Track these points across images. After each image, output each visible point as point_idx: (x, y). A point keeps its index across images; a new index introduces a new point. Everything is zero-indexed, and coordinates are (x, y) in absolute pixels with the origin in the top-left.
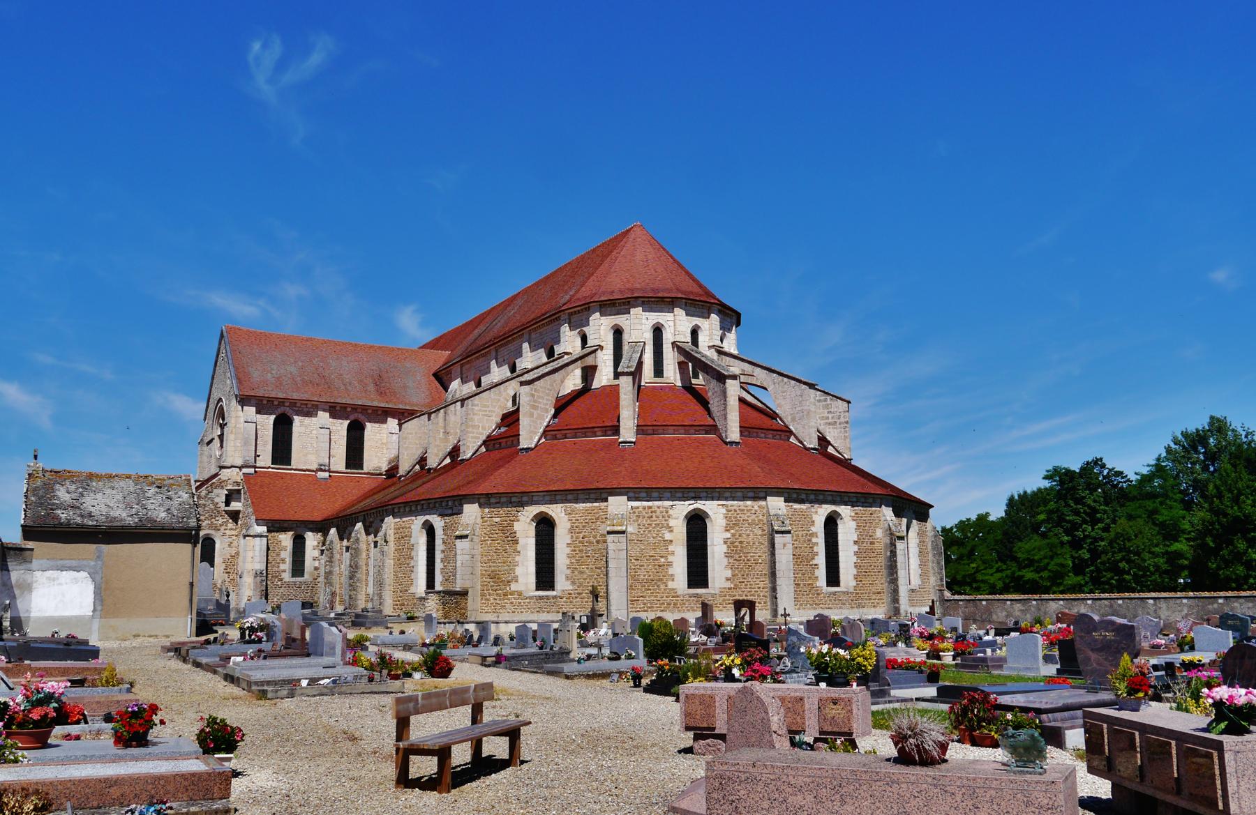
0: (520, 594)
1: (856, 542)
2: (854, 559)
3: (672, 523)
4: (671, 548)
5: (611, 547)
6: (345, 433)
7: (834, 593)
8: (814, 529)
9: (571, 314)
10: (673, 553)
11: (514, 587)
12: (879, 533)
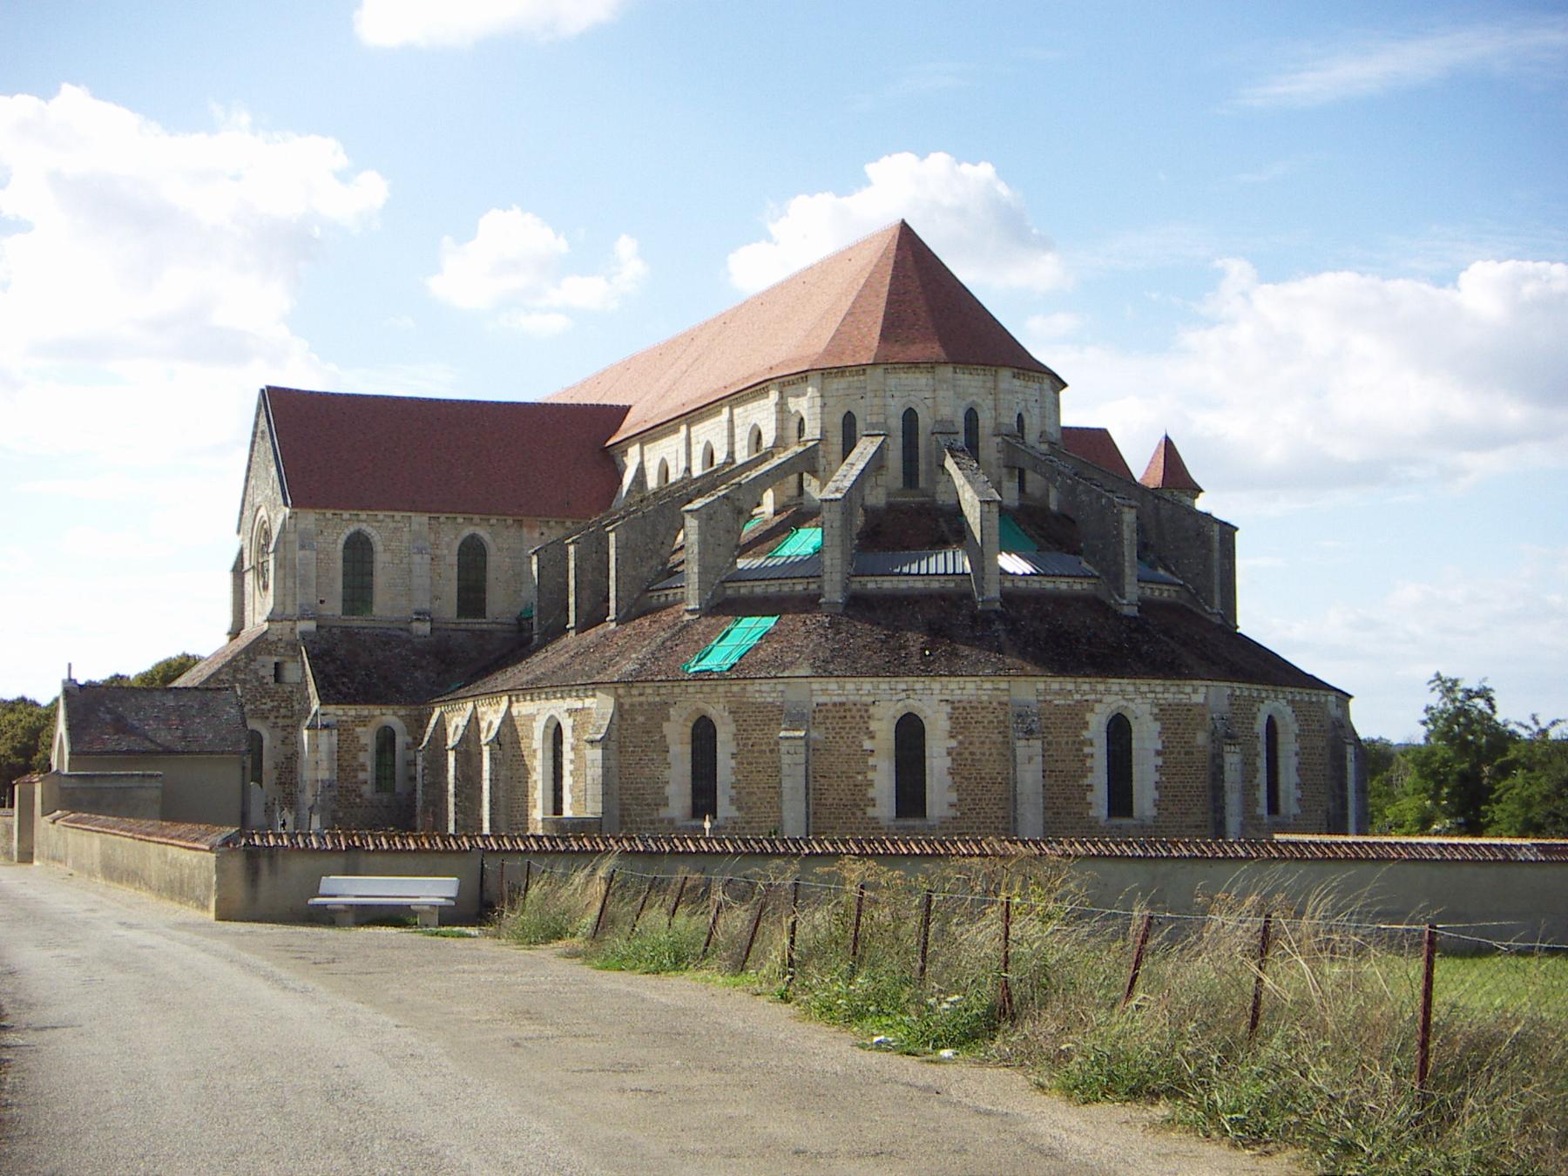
0: (671, 821)
1: (1158, 753)
2: (1156, 777)
3: (873, 726)
4: (871, 761)
5: (786, 759)
6: (454, 560)
7: (1119, 827)
8: (1086, 734)
9: (783, 385)
10: (874, 768)
11: (664, 813)
12: (1201, 738)
